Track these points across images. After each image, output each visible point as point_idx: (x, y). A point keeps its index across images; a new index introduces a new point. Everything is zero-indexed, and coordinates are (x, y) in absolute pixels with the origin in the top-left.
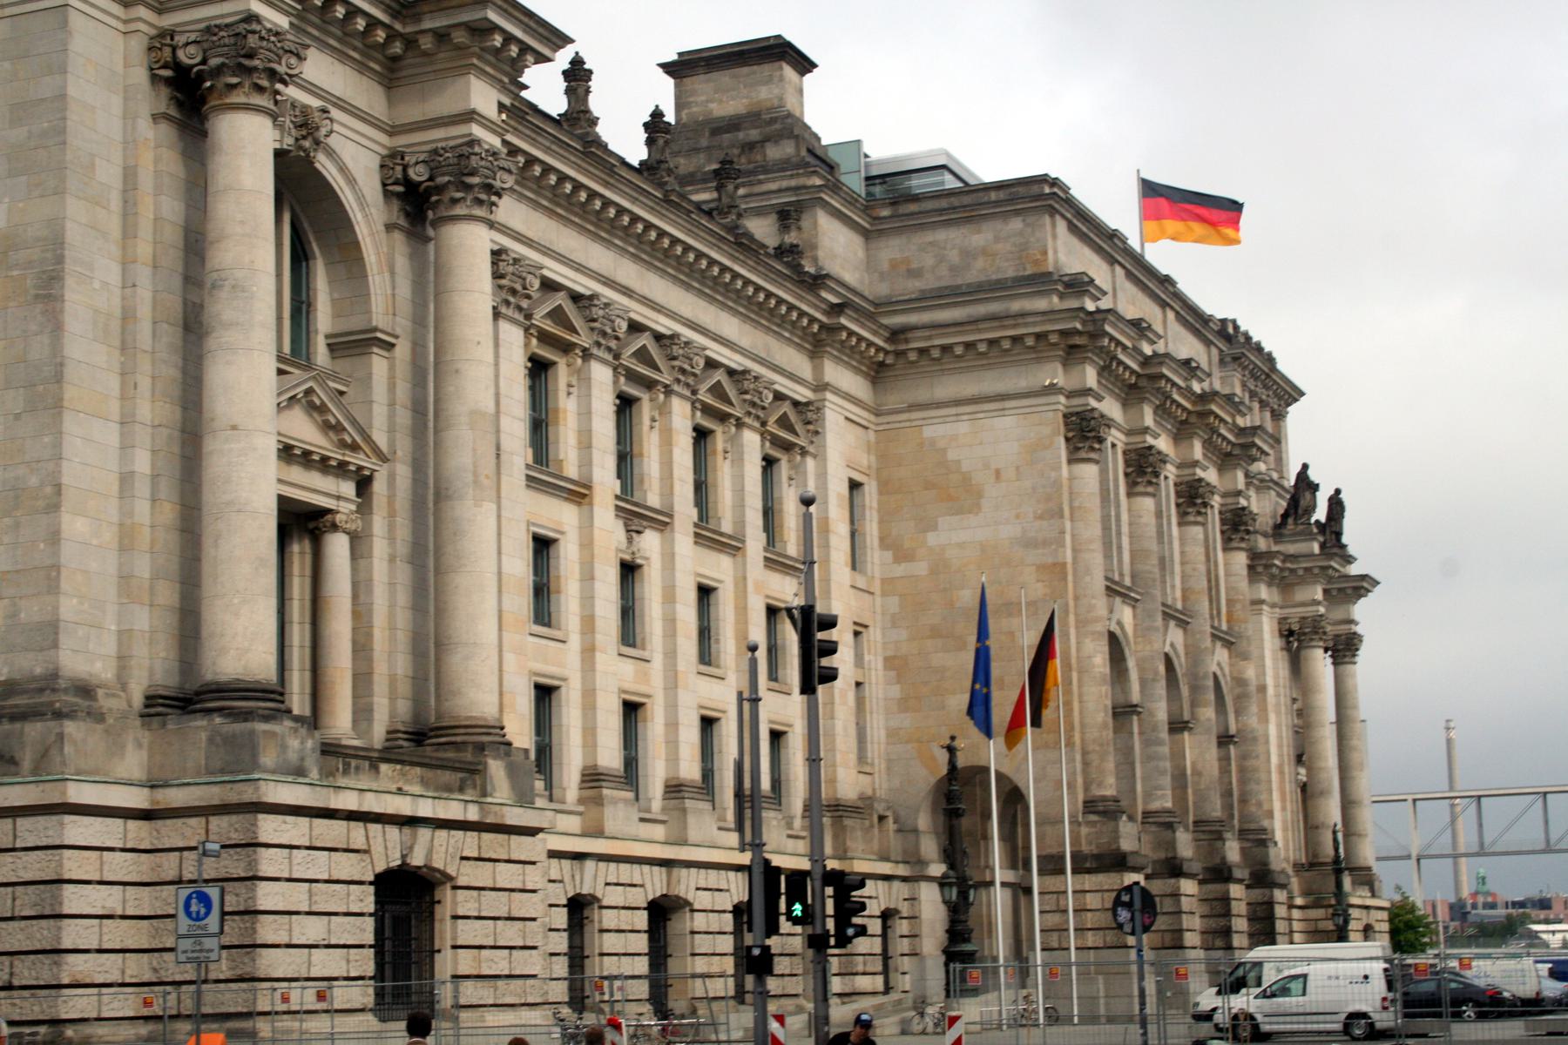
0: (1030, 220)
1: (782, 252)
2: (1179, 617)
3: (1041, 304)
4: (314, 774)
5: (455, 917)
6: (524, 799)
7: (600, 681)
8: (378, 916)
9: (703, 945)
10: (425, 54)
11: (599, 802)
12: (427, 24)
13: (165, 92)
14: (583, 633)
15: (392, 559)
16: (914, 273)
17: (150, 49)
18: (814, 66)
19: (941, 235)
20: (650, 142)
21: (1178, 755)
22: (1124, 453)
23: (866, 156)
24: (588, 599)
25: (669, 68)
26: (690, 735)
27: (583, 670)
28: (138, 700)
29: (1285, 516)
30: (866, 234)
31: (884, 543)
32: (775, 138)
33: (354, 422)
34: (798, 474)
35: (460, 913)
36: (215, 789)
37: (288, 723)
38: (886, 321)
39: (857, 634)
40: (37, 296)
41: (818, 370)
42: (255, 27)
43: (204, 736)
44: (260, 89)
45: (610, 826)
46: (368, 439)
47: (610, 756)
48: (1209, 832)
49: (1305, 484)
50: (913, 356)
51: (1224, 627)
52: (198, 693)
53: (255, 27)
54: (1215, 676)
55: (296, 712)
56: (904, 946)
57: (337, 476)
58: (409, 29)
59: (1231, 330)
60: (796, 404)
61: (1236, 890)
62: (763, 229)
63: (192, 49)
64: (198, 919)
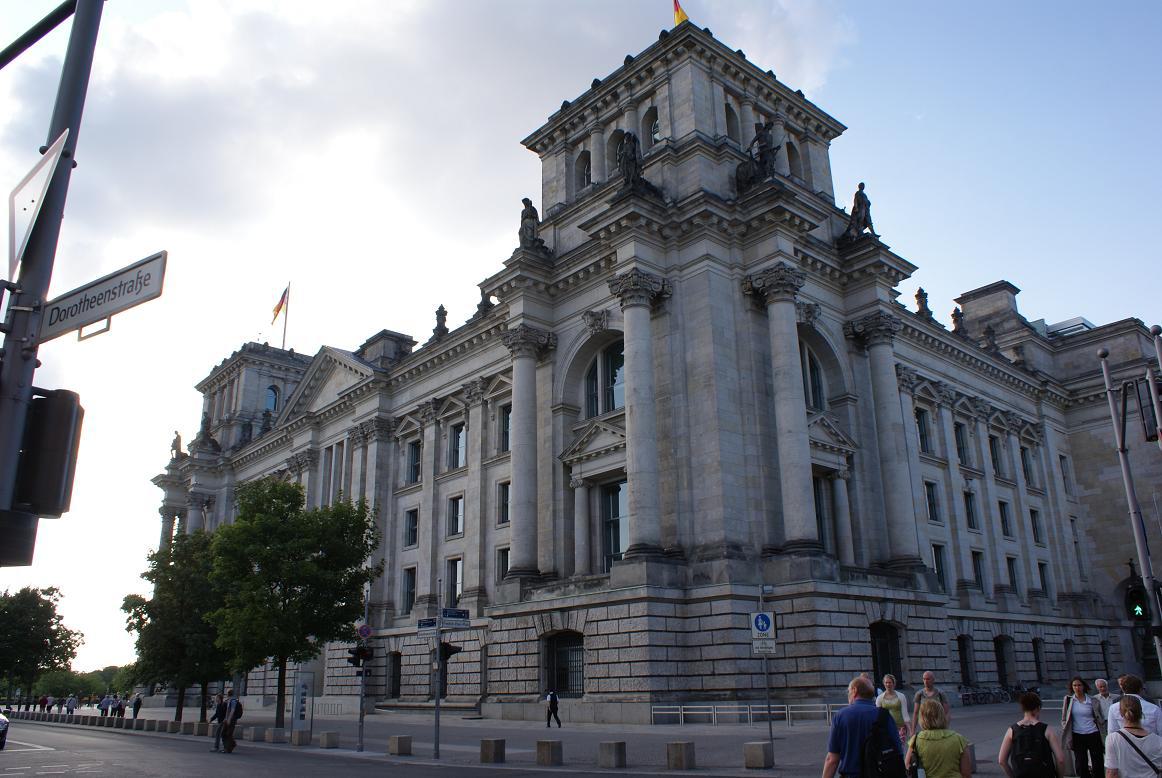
0: (1128, 337)
4: (838, 580)
5: (909, 643)
6: (934, 591)
7: (961, 543)
8: (873, 643)
9: (1021, 656)
10: (857, 280)
11: (967, 594)
12: (856, 268)
13: (748, 300)
14: (951, 523)
15: (864, 490)
17: (742, 284)
18: (1019, 291)
19: (1086, 350)
20: (955, 321)
24: (952, 509)
26: (1003, 565)
27: (953, 539)
30: (1052, 354)
31: (1079, 481)
32: (1007, 320)
33: (842, 432)
34: (1036, 455)
35: (911, 641)
36: (795, 587)
37: (824, 557)
38: (1068, 388)
39: (1072, 521)
40: (706, 386)
41: (1039, 410)
42: (781, 267)
43: (788, 564)
44: (787, 292)
45: (972, 605)
46: (849, 438)
47: (969, 574)
50: (1081, 401)
52: (784, 547)
53: (781, 267)
55: (829, 552)
56: (1112, 658)
57: (838, 455)
58: (849, 271)
60: (1032, 424)
62: (1011, 356)
63: (758, 281)
64: (763, 630)
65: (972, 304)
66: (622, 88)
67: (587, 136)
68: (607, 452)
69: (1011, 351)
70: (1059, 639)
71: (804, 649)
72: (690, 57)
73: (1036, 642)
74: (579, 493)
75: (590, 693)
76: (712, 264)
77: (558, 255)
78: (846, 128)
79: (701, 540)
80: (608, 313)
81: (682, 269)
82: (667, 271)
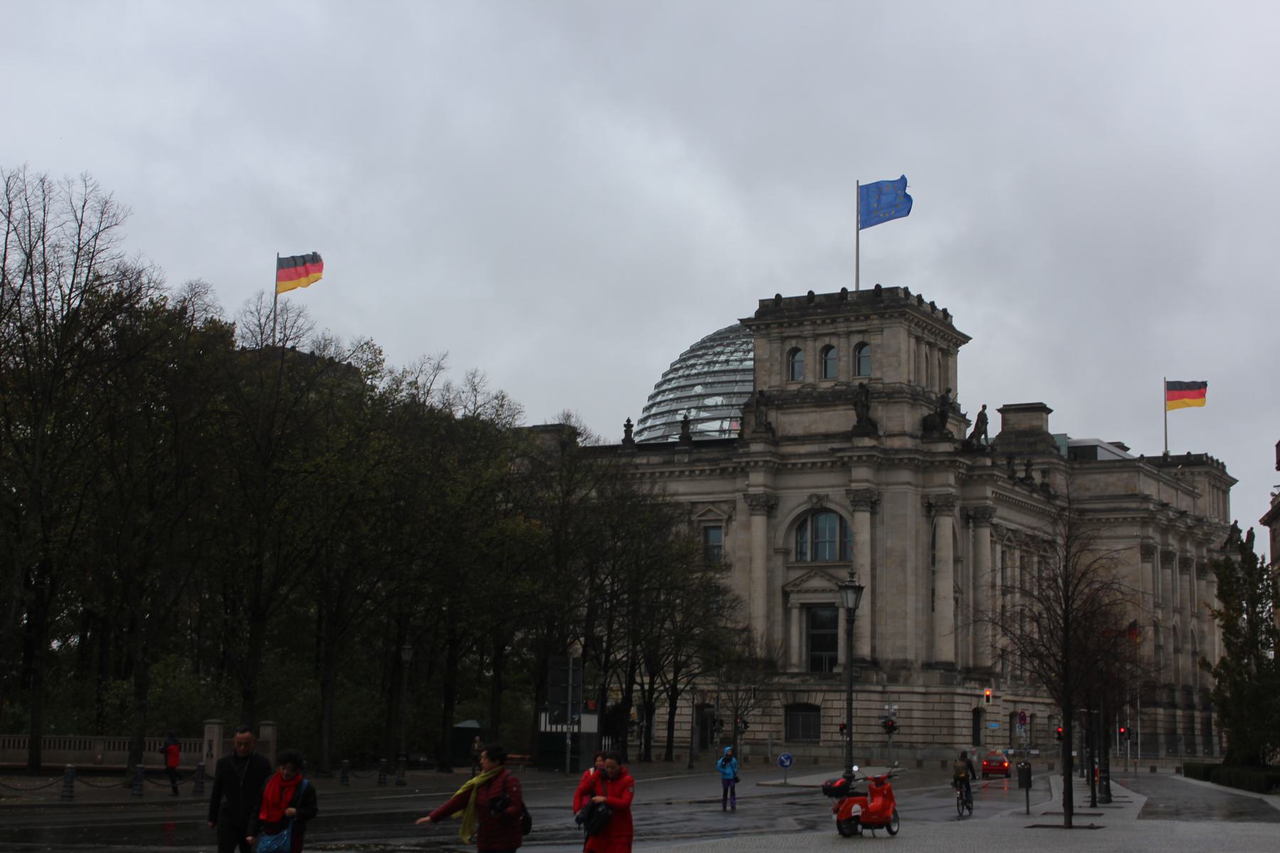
0: (1131, 474)
1: (1043, 485)
2: (1179, 611)
3: (1134, 505)
16: (1088, 489)
19: (1097, 477)
21: (1176, 661)
22: (1161, 552)
23: (1069, 438)
25: (999, 410)
28: (920, 665)
29: (1226, 543)
48: (1188, 690)
49: (1235, 530)
51: (1196, 611)
54: (1192, 630)
59: (1205, 459)
61: (1197, 714)
65: (1012, 417)
66: (842, 320)
67: (805, 338)
68: (823, 591)
69: (1039, 472)
70: (1046, 714)
71: (945, 723)
72: (901, 323)
73: (1033, 716)
74: (795, 613)
75: (825, 741)
76: (909, 487)
77: (780, 434)
78: (971, 339)
79: (891, 657)
80: (827, 495)
81: (888, 484)
82: (879, 484)
